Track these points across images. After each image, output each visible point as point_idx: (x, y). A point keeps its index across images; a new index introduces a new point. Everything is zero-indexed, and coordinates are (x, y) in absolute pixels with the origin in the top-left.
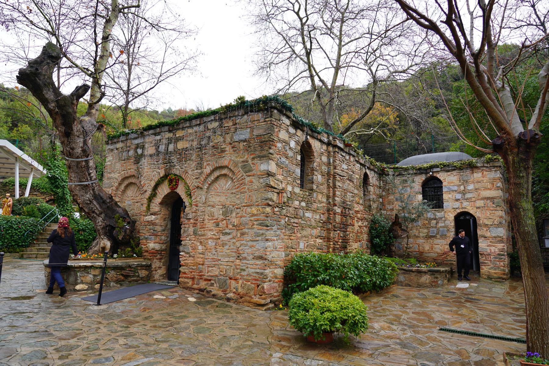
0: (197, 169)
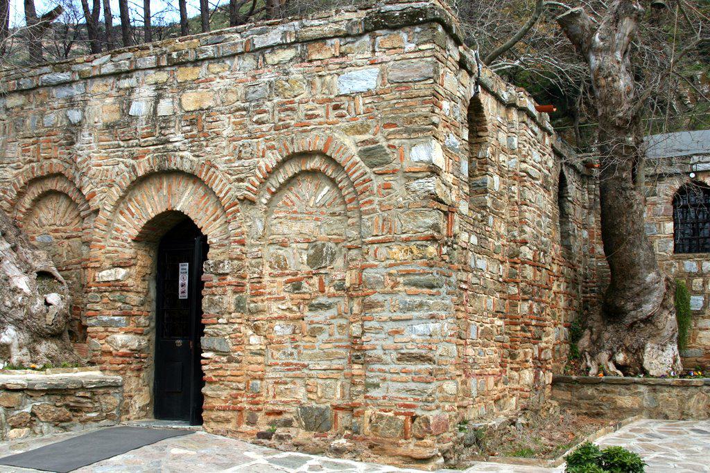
0: (240, 158)
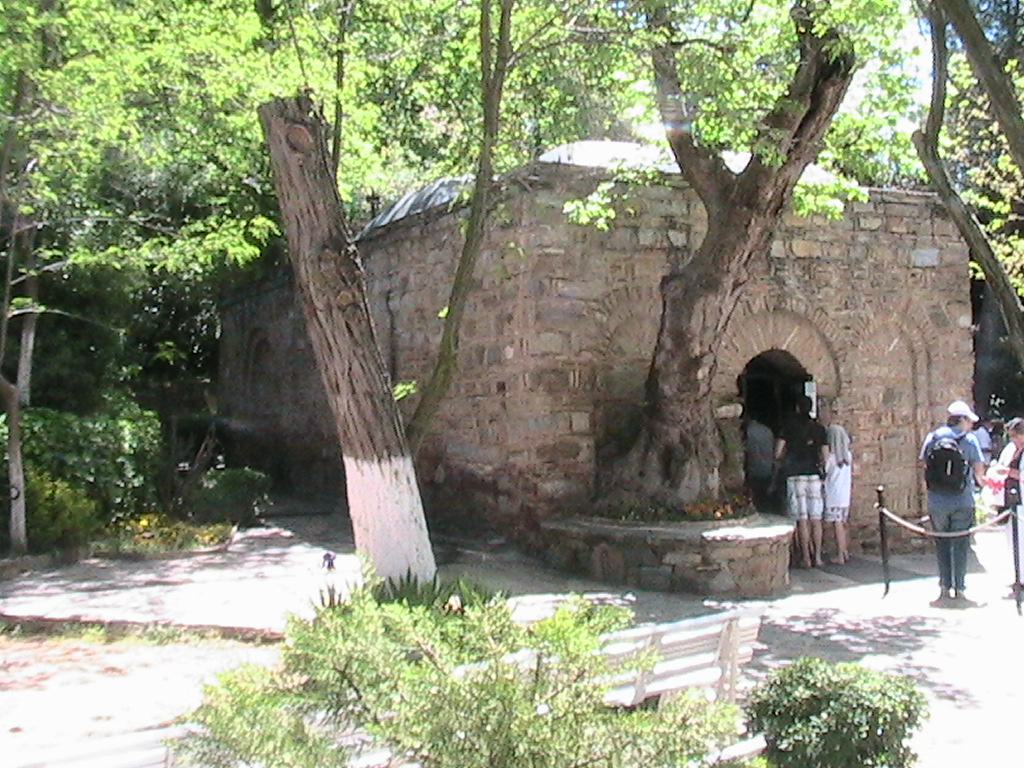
0: (847, 308)
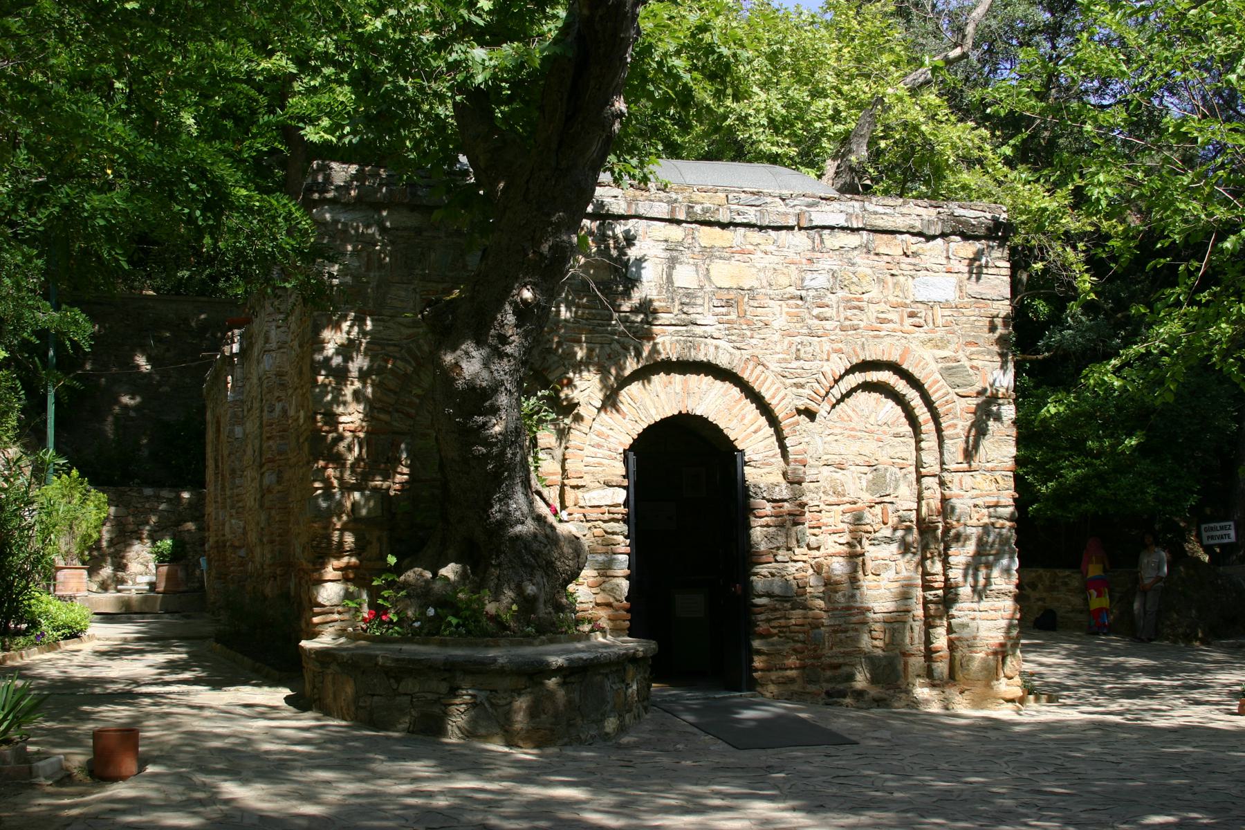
0: (798, 358)
